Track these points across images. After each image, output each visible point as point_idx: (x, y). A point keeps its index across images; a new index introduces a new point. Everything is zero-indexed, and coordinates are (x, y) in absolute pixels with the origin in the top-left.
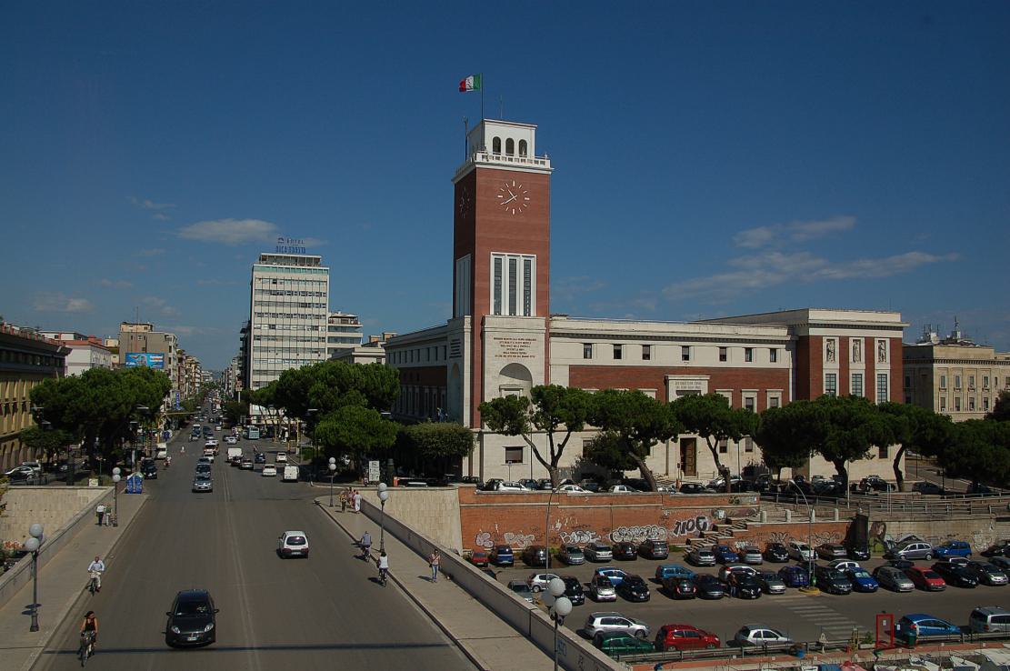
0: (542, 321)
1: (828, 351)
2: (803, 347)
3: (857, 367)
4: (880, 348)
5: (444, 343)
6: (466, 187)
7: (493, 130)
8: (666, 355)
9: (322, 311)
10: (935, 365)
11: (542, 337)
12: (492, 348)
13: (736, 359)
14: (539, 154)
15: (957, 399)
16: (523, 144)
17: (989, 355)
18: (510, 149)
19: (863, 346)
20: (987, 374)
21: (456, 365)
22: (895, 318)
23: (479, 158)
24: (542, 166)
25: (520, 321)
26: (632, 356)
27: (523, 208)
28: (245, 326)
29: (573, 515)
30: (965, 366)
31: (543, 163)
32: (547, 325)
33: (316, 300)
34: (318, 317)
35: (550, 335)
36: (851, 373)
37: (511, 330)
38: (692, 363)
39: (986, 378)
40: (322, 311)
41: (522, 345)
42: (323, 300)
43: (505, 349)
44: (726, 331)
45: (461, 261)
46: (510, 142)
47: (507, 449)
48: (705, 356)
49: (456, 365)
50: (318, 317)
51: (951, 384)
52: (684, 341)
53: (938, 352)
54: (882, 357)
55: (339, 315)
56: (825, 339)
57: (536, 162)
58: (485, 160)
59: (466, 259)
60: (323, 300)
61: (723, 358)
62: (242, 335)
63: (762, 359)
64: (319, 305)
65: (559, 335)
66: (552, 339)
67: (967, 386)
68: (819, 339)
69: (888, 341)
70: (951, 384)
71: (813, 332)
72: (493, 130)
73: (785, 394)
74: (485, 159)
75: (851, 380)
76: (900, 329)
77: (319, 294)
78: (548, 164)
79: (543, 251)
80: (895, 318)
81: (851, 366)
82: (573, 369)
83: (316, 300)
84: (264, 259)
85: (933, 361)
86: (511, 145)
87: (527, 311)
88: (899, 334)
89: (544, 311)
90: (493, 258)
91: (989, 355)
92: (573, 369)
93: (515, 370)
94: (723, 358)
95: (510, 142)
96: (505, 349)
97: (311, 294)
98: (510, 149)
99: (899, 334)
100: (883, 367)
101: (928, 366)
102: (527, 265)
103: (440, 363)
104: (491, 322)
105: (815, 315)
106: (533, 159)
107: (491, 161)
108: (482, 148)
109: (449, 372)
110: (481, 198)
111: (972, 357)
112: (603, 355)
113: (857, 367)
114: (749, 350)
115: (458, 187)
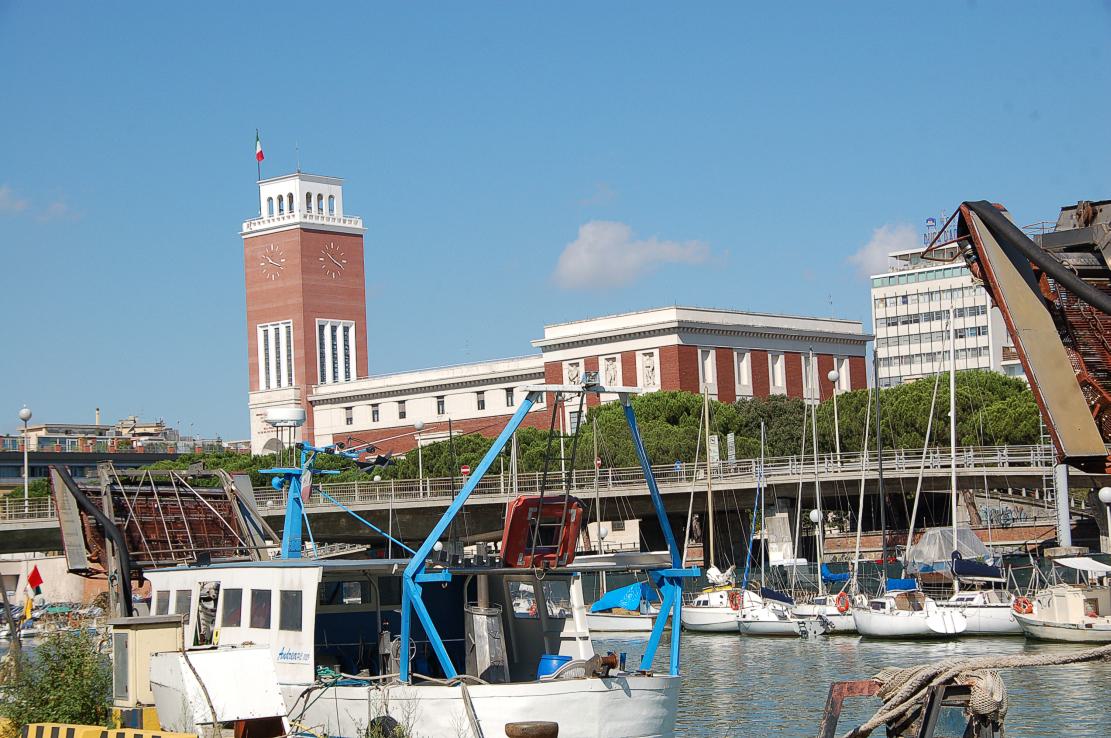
7: (270, 190)
19: (618, 365)
26: (389, 417)
46: (280, 198)
52: (402, 395)
56: (565, 365)
58: (249, 230)
61: (481, 405)
66: (316, 408)
82: (336, 437)
92: (336, 437)
94: (481, 405)
95: (280, 198)
108: (258, 216)
112: (363, 420)
114: (509, 391)
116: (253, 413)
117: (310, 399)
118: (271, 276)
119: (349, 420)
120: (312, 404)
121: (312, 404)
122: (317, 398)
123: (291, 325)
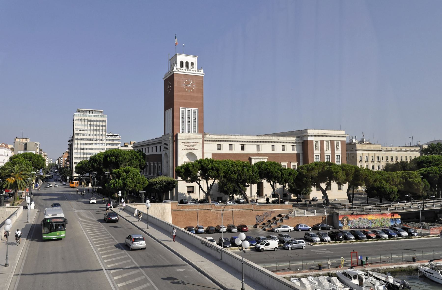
0: (201, 135)
1: (316, 146)
2: (305, 146)
3: (328, 153)
4: (337, 145)
5: (160, 145)
6: (170, 81)
8: (250, 149)
9: (104, 133)
10: (357, 152)
11: (201, 142)
12: (181, 146)
13: (278, 150)
14: (199, 67)
15: (367, 166)
16: (192, 64)
17: (379, 148)
18: (187, 66)
19: (330, 144)
20: (379, 156)
21: (166, 153)
22: (342, 133)
23: (175, 68)
24: (199, 73)
25: (192, 135)
26: (237, 149)
27: (193, 90)
28: (71, 139)
29: (217, 213)
30: (370, 152)
31: (201, 72)
32: (203, 137)
33: (101, 128)
34: (102, 135)
35: (204, 141)
36: (325, 155)
37: (189, 139)
38: (261, 152)
39: (378, 158)
40: (104, 133)
41: (192, 146)
42: (104, 128)
43: (186, 147)
44: (274, 139)
45: (167, 111)
46: (187, 63)
47: (188, 187)
48: (266, 149)
49: (166, 153)
50: (102, 135)
51: (364, 160)
53: (358, 147)
54: (338, 149)
55: (111, 134)
57: (198, 71)
58: (177, 70)
59: (170, 110)
60: (104, 128)
62: (69, 143)
63: (289, 150)
64: (102, 130)
65: (207, 141)
66: (205, 142)
67: (370, 160)
68: (312, 141)
69: (340, 142)
70: (364, 160)
71: (309, 138)
72: (180, 58)
73: (298, 164)
74: (177, 70)
75: (325, 158)
76: (345, 137)
77: (102, 126)
78: (202, 71)
79: (200, 106)
80: (342, 133)
81: (325, 152)
82: (213, 154)
83: (101, 128)
84: (79, 111)
85: (356, 150)
86: (188, 65)
87: (195, 132)
88: (344, 139)
89: (201, 131)
90: (181, 110)
91: (379, 148)
92: (213, 154)
93: (191, 155)
94: (273, 150)
95: (187, 63)
96: (186, 147)
97: (99, 126)
98: (187, 66)
99: (344, 139)
100: (338, 153)
101: (354, 152)
102: (195, 112)
103: (158, 153)
104: (180, 136)
105: (310, 132)
106: (196, 70)
107: (180, 71)
109: (163, 156)
110: (176, 85)
111: (372, 149)
112: (225, 149)
113: (328, 153)
114: (283, 146)
115: (166, 81)
116: (179, 141)
117: (205, 139)
118: (188, 91)
119: (219, 149)
120: (205, 140)
121: (205, 140)
122: (206, 139)
123: (197, 110)
